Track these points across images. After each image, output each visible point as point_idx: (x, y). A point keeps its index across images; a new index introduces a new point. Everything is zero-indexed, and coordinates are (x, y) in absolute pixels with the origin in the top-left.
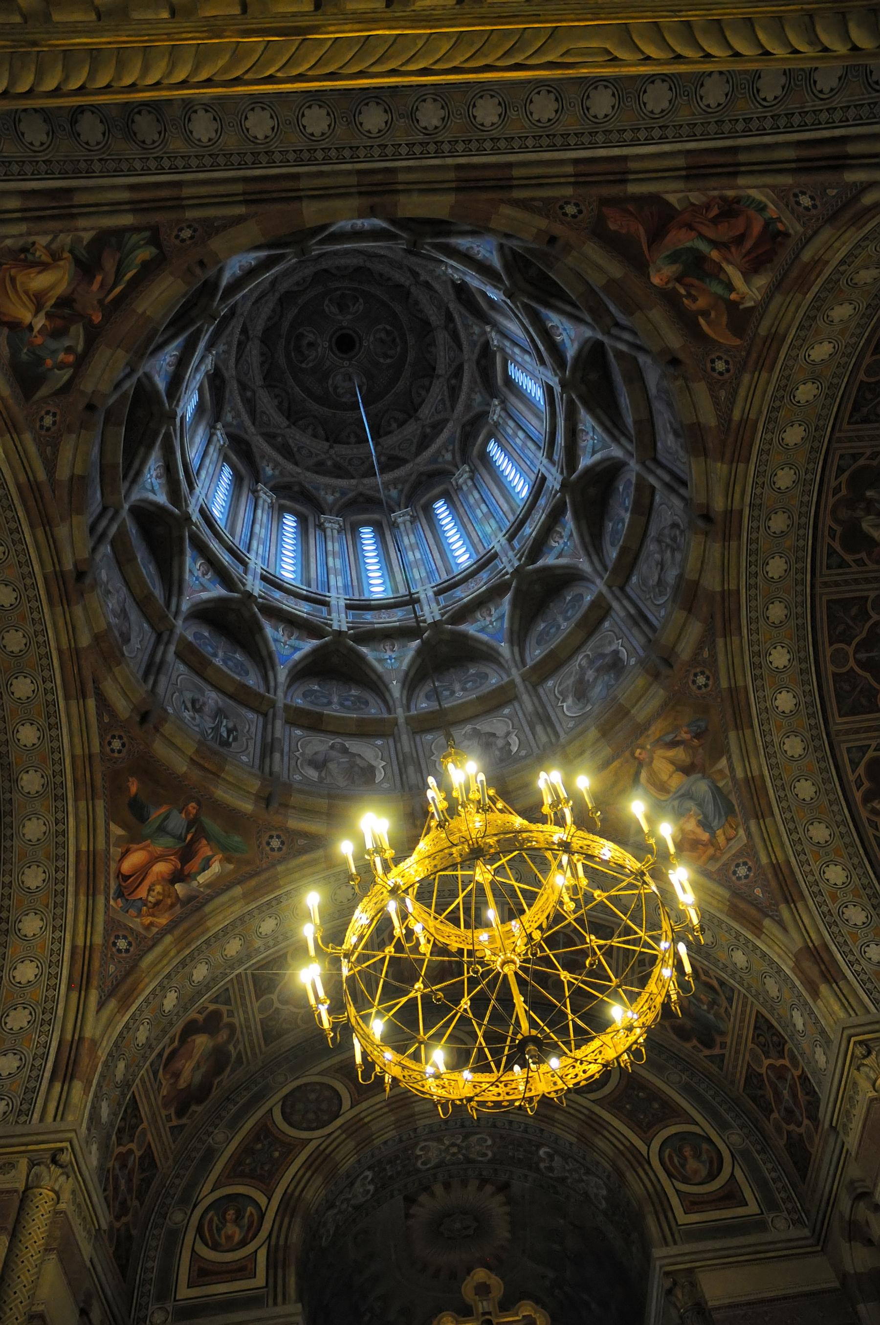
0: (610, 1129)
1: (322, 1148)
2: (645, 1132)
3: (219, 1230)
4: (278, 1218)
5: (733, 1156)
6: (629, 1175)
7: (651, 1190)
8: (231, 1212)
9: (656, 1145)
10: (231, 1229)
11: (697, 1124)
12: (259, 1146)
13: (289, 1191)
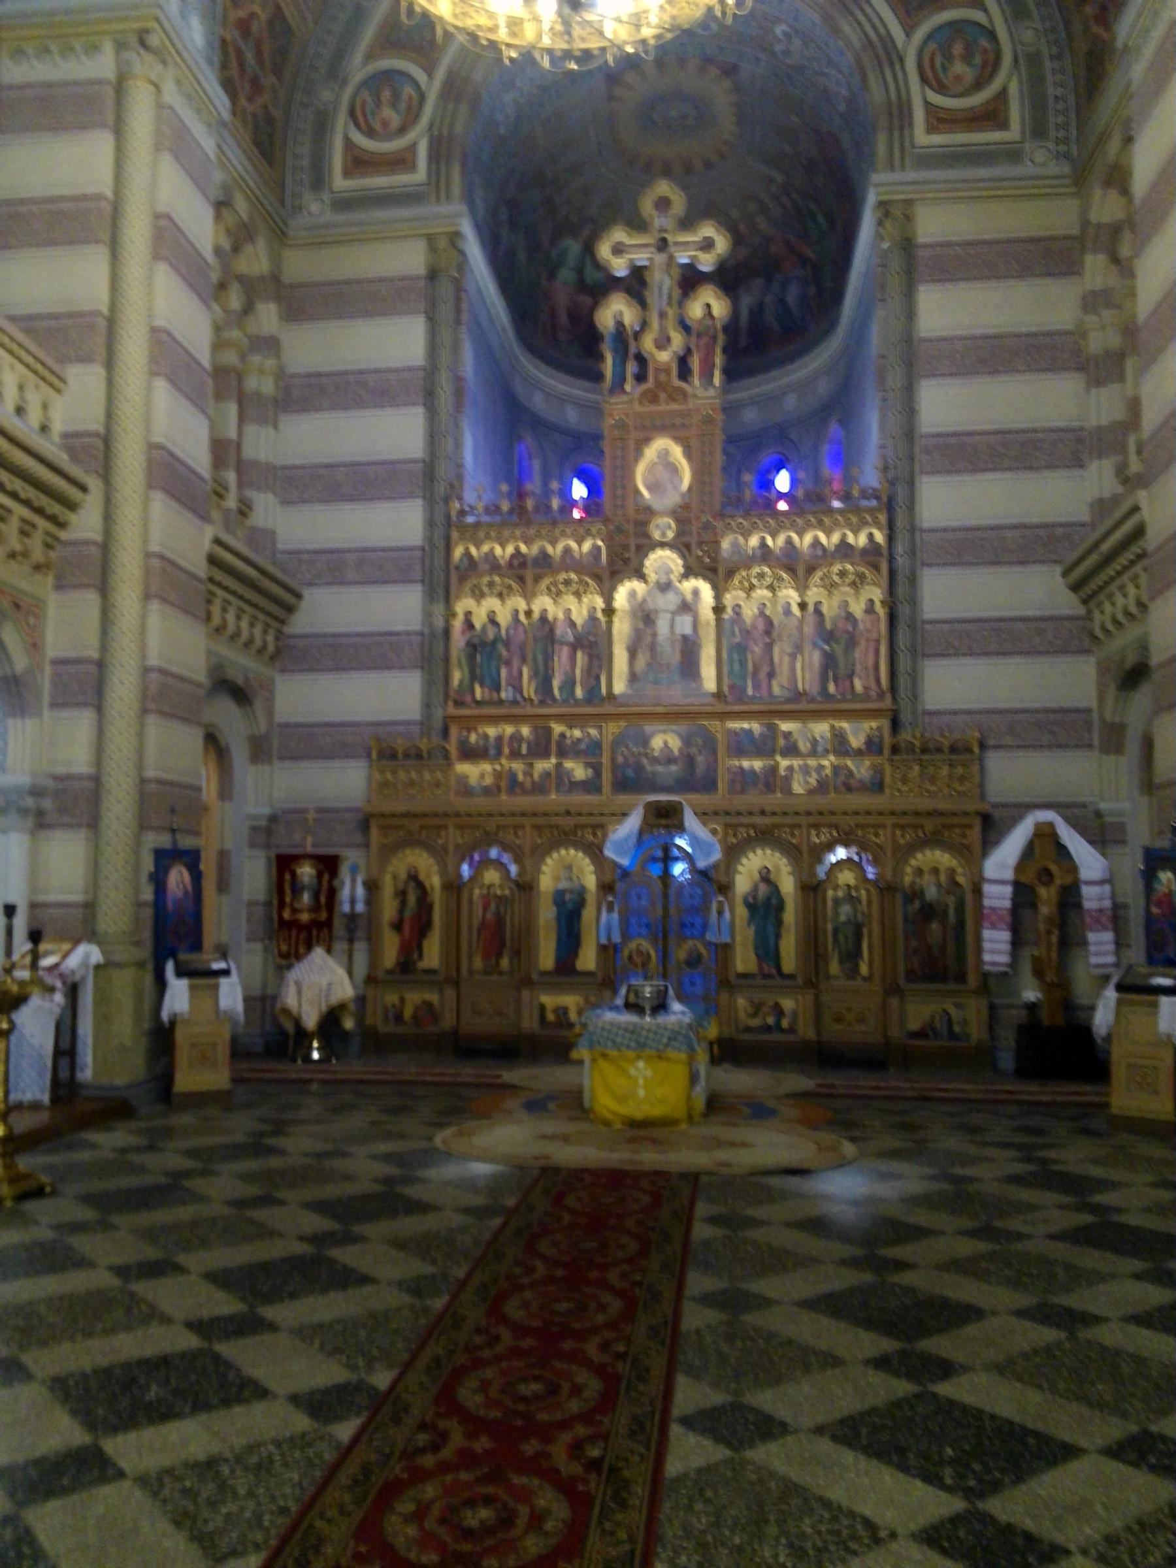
3: (373, 114)
5: (1016, 60)
7: (894, 97)
9: (919, 35)
11: (985, 10)
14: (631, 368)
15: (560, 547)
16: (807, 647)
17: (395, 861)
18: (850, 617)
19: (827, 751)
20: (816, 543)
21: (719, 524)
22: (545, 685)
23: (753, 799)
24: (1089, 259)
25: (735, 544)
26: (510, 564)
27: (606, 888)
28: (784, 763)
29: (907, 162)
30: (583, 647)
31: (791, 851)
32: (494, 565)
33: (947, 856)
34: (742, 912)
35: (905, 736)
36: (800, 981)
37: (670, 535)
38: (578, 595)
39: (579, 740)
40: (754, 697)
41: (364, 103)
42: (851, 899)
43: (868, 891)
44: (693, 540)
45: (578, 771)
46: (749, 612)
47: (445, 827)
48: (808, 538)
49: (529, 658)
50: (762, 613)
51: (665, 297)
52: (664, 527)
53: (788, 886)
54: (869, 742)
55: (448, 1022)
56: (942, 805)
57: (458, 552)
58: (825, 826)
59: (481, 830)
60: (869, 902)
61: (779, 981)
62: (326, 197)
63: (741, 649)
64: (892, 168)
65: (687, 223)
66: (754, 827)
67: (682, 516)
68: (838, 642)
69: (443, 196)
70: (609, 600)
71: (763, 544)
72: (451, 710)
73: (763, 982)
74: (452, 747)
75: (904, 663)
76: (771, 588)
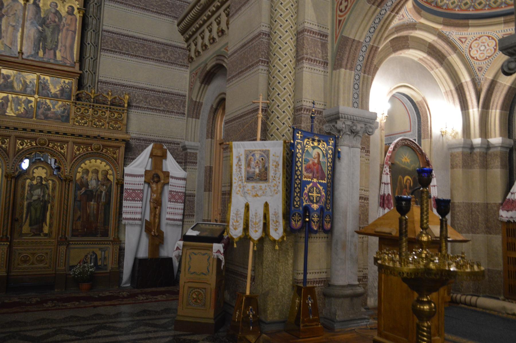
18: (57, 13)
19: (34, 93)
33: (104, 163)
35: (85, 91)
42: (41, 185)
43: (53, 181)
54: (62, 90)
58: (27, 138)
60: (54, 189)
68: (48, 27)
75: (89, 52)
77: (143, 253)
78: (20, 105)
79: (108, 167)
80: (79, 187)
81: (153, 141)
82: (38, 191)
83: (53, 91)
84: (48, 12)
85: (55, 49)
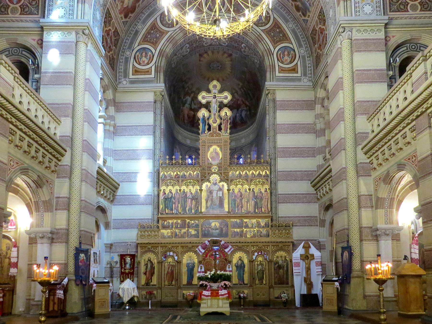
0: (264, 41)
1: (172, 35)
2: (275, 44)
4: (158, 57)
6: (266, 58)
7: (271, 64)
8: (144, 53)
10: (144, 59)
12: (152, 32)
13: (162, 49)
14: (207, 127)
15: (188, 173)
16: (251, 200)
17: (144, 256)
20: (253, 173)
21: (229, 168)
22: (184, 209)
23: (237, 239)
24: (317, 106)
25: (233, 173)
26: (175, 177)
27: (200, 262)
28: (245, 230)
29: (274, 79)
30: (194, 199)
31: (247, 252)
32: (171, 178)
33: (284, 253)
34: (234, 268)
35: (274, 223)
36: (249, 285)
37: (217, 170)
38: (193, 185)
39: (193, 224)
40: (237, 212)
41: (138, 56)
42: (261, 264)
44: (223, 171)
45: (193, 232)
46: (236, 191)
47: (158, 247)
48: (251, 172)
49: (180, 202)
50: (239, 191)
51: (215, 111)
52: (215, 169)
53: (246, 261)
54: (266, 224)
55: (159, 299)
56: (284, 240)
57: (161, 174)
59: (167, 248)
61: (243, 286)
62: (127, 80)
63: (235, 200)
64: (270, 81)
65: (221, 91)
66: (237, 246)
67: (219, 166)
69: (158, 81)
70: (201, 187)
71: (240, 173)
72: (160, 216)
73: (239, 286)
74: (160, 225)
76: (242, 185)
77: (305, 292)
78: (251, 233)
79: (286, 254)
80: (275, 264)
81: (304, 240)
82: (260, 267)
83: (262, 225)
84: (257, 193)
85: (262, 208)
